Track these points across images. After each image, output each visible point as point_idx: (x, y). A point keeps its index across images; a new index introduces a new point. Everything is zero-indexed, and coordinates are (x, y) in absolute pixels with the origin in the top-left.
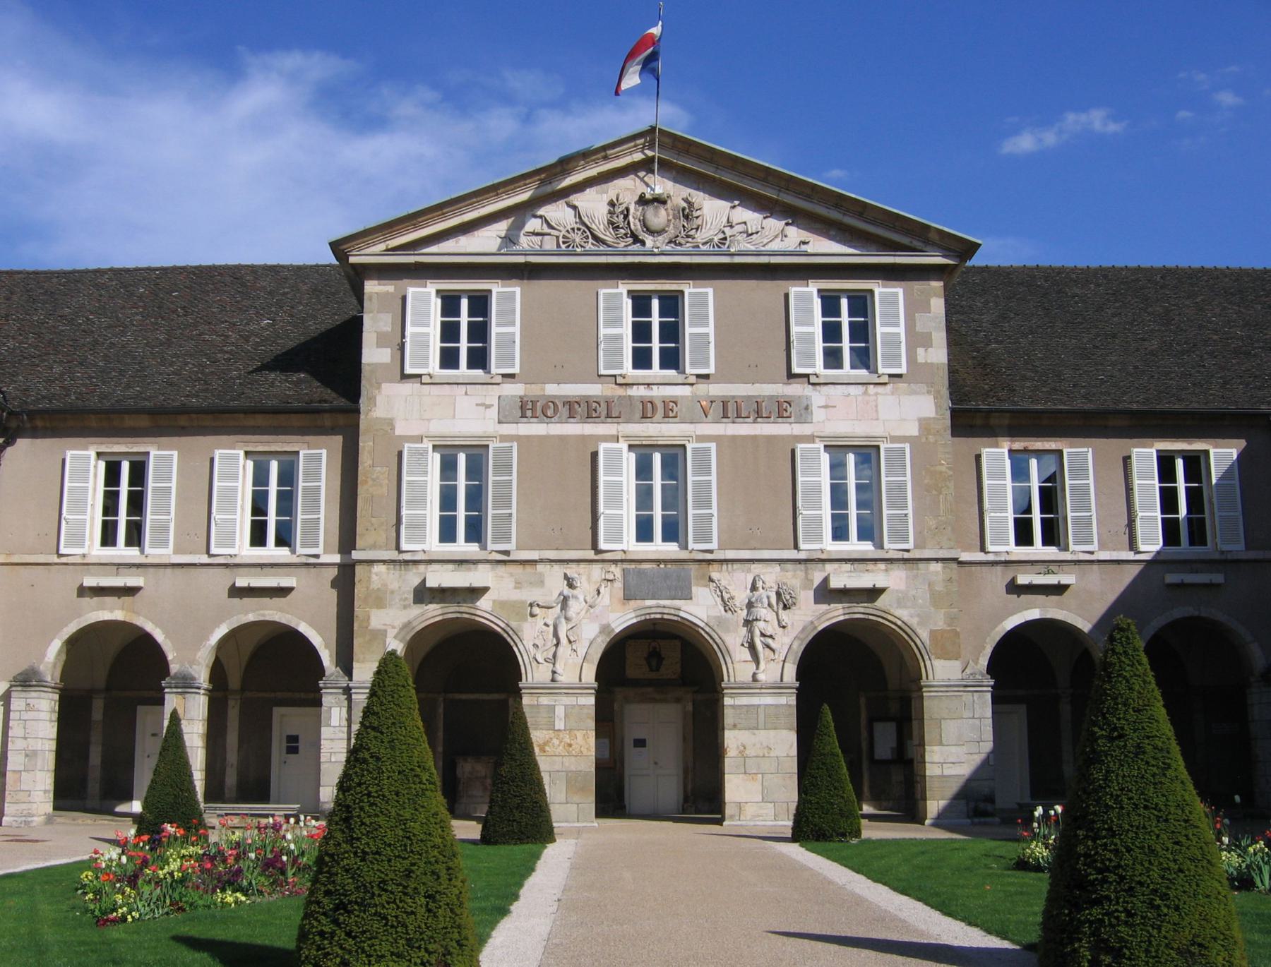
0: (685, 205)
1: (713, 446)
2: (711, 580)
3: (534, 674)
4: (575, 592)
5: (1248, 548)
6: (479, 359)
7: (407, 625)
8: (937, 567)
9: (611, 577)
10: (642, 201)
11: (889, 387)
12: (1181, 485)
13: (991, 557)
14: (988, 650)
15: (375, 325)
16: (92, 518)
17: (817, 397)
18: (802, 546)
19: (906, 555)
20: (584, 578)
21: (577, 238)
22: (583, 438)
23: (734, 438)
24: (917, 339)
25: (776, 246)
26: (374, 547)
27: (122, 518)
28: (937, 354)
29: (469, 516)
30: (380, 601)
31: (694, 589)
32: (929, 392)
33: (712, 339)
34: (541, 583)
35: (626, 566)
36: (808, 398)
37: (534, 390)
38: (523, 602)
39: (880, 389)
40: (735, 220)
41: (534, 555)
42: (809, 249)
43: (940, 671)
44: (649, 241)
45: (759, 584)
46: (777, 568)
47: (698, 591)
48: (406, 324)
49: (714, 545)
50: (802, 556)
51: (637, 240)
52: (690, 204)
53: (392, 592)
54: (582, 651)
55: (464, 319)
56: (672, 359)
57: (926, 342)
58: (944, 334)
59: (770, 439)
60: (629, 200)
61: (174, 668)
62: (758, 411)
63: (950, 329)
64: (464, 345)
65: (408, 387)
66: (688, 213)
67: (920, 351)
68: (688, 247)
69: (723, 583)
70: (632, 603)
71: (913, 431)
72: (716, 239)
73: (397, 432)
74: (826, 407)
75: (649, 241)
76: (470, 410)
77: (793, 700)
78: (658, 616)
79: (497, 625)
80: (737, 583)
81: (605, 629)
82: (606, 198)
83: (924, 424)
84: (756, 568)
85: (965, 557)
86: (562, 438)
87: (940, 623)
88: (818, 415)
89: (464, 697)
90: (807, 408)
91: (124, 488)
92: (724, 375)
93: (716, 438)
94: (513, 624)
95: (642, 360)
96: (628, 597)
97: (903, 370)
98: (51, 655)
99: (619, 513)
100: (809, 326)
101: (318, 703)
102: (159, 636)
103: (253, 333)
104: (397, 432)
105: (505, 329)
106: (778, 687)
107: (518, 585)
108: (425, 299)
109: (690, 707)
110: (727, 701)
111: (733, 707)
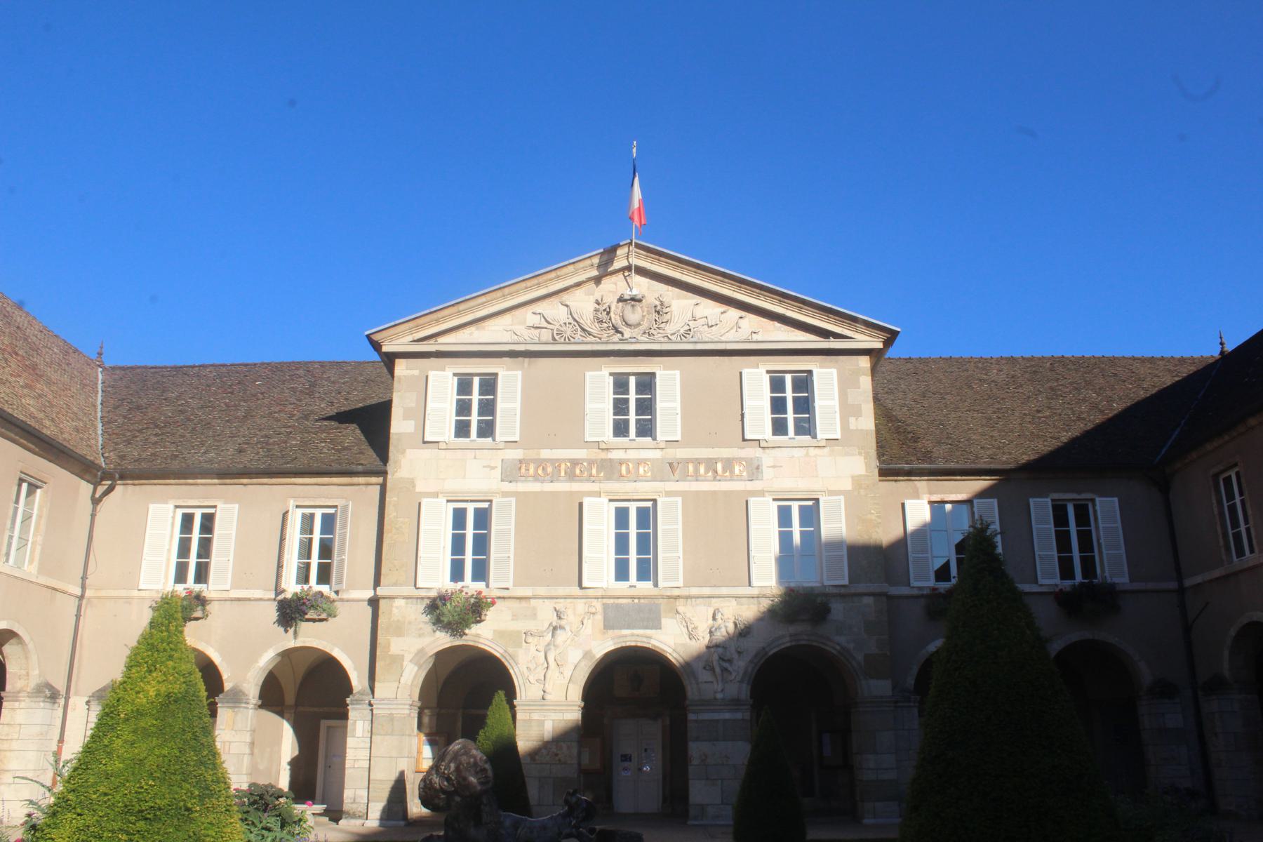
0: (658, 303)
1: (679, 499)
2: (677, 612)
3: (526, 691)
4: (563, 623)
5: (1131, 580)
6: (487, 430)
7: (421, 652)
8: (868, 600)
9: (593, 610)
10: (621, 300)
11: (826, 450)
12: (1073, 528)
13: (915, 592)
16: (168, 560)
17: (767, 459)
18: (754, 583)
19: (843, 591)
20: (570, 612)
21: (568, 331)
22: (571, 493)
24: (848, 410)
25: (731, 336)
26: (395, 584)
27: (193, 560)
28: (867, 422)
30: (399, 630)
31: (664, 621)
32: (860, 454)
33: (679, 410)
34: (534, 616)
35: (605, 601)
36: (758, 459)
37: (532, 454)
38: (519, 632)
39: (818, 451)
40: (698, 315)
44: (628, 333)
45: (718, 616)
46: (733, 602)
47: (667, 622)
48: (425, 402)
49: (680, 584)
50: (755, 592)
51: (618, 331)
52: (662, 304)
53: (410, 623)
54: (568, 674)
55: (475, 397)
56: (646, 429)
57: (857, 413)
58: (871, 405)
60: (611, 300)
61: (227, 686)
63: (876, 399)
64: (474, 418)
65: (427, 453)
66: (660, 310)
67: (852, 420)
68: (659, 337)
69: (688, 615)
70: (610, 632)
71: (848, 485)
72: (682, 331)
73: (418, 489)
74: (774, 467)
75: (628, 333)
76: (476, 472)
77: (747, 716)
78: (633, 644)
79: (497, 651)
81: (587, 654)
82: (592, 299)
83: (856, 480)
84: (716, 603)
85: (895, 591)
86: (554, 494)
88: (767, 473)
89: (316, 709)
90: (758, 468)
91: (196, 535)
92: (688, 440)
93: (683, 494)
94: (510, 650)
95: (620, 429)
97: (838, 436)
101: (344, 716)
103: (312, 412)
104: (418, 489)
105: (509, 403)
106: (735, 703)
107: (515, 617)
108: (442, 383)
109: (668, 722)
110: (691, 717)
111: (696, 721)
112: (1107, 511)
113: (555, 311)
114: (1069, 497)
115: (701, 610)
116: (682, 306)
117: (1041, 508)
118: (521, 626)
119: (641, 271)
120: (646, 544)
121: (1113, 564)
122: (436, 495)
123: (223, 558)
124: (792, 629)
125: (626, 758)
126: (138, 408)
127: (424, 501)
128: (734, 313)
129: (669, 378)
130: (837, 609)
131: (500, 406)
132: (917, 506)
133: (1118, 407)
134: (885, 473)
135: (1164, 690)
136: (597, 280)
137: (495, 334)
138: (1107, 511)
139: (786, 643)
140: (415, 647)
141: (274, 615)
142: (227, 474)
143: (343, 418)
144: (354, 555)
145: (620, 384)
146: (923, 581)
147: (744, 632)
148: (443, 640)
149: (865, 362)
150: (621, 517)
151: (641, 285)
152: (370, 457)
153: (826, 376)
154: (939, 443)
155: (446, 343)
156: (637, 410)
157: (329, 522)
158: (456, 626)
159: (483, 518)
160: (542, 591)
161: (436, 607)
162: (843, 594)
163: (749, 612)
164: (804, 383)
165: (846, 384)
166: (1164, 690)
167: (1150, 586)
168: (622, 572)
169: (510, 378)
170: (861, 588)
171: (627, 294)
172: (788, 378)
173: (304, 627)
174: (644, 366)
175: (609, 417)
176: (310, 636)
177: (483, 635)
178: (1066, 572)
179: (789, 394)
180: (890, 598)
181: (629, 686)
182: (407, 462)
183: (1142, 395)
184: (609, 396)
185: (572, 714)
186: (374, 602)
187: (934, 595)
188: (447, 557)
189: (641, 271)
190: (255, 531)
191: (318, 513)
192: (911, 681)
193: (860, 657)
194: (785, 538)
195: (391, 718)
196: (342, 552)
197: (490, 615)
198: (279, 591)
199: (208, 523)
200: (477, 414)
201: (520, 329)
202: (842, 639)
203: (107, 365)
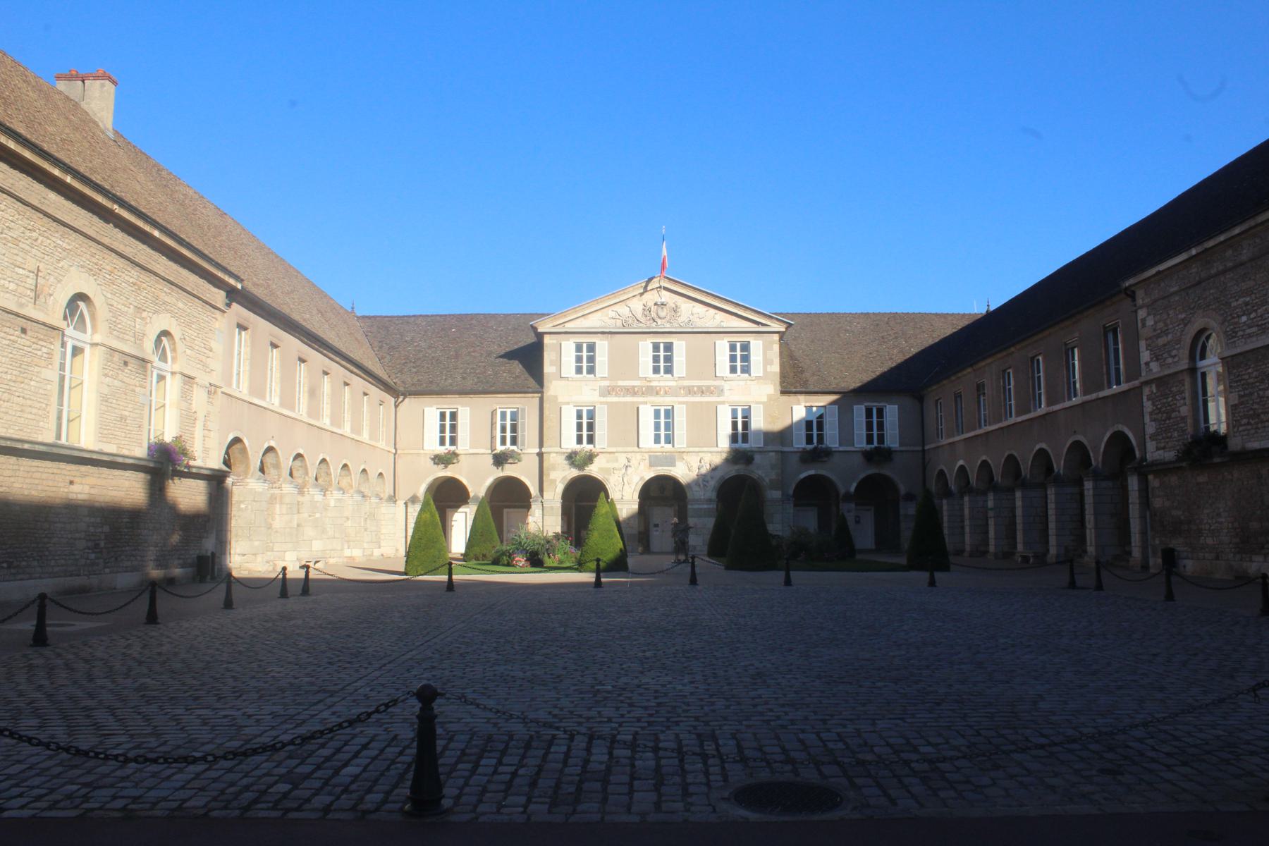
3: (614, 494)
5: (901, 445)
6: (591, 370)
12: (875, 420)
14: (794, 486)
17: (726, 386)
22: (633, 403)
23: (693, 403)
24: (767, 362)
28: (775, 368)
30: (554, 468)
34: (617, 460)
37: (614, 383)
41: (613, 449)
42: (724, 324)
44: (659, 322)
48: (560, 358)
56: (669, 370)
57: (771, 363)
59: (708, 403)
60: (651, 304)
61: (472, 495)
62: (702, 391)
64: (585, 364)
65: (563, 383)
71: (765, 399)
75: (659, 322)
79: (600, 477)
83: (770, 397)
85: (786, 449)
87: (773, 475)
88: (726, 393)
91: (448, 423)
92: (688, 377)
95: (656, 370)
96: (651, 465)
98: (421, 491)
101: (528, 507)
102: (465, 482)
104: (560, 399)
106: (710, 500)
108: (569, 346)
112: (892, 412)
113: (623, 310)
114: (875, 405)
115: (697, 458)
116: (686, 307)
117: (859, 411)
118: (611, 465)
119: (666, 289)
120: (669, 426)
121: (892, 440)
122: (568, 403)
123: (466, 435)
124: (737, 467)
125: (656, 526)
126: (393, 348)
127: (564, 407)
128: (712, 311)
129: (680, 346)
130: (757, 458)
131: (598, 359)
132: (799, 410)
133: (914, 351)
134: (783, 392)
135: (910, 497)
136: (642, 294)
137: (593, 322)
138: (892, 412)
139: (733, 473)
140: (561, 475)
141: (491, 461)
142: (463, 392)
143: (510, 355)
144: (529, 431)
145: (656, 347)
146: (800, 443)
147: (714, 469)
148: (574, 473)
149: (776, 337)
150: (657, 413)
151: (666, 297)
152: (531, 382)
153: (756, 345)
154: (813, 374)
155: (570, 326)
156: (664, 360)
157: (514, 417)
158: (581, 467)
159: (591, 415)
160: (620, 449)
161: (571, 458)
162: (761, 451)
163: (718, 459)
164: (746, 347)
165: (766, 348)
166: (910, 497)
167: (912, 448)
168: (657, 440)
169: (602, 345)
170: (769, 448)
171: (659, 301)
172: (738, 345)
173: (507, 466)
174: (668, 339)
175: (651, 364)
176: (509, 471)
177: (593, 470)
178: (870, 439)
179: (738, 353)
180: (782, 452)
181: (661, 492)
182: (553, 388)
183: (931, 342)
184: (651, 353)
185: (635, 507)
186: (540, 455)
187: (804, 452)
188: (574, 433)
189: (666, 289)
190: (476, 418)
191: (508, 412)
192: (791, 492)
193: (767, 480)
194: (735, 425)
195: (552, 508)
196: (523, 431)
197: (596, 460)
198: (493, 449)
199: (454, 416)
200: (587, 362)
201: (606, 319)
202: (760, 472)
203: (359, 314)
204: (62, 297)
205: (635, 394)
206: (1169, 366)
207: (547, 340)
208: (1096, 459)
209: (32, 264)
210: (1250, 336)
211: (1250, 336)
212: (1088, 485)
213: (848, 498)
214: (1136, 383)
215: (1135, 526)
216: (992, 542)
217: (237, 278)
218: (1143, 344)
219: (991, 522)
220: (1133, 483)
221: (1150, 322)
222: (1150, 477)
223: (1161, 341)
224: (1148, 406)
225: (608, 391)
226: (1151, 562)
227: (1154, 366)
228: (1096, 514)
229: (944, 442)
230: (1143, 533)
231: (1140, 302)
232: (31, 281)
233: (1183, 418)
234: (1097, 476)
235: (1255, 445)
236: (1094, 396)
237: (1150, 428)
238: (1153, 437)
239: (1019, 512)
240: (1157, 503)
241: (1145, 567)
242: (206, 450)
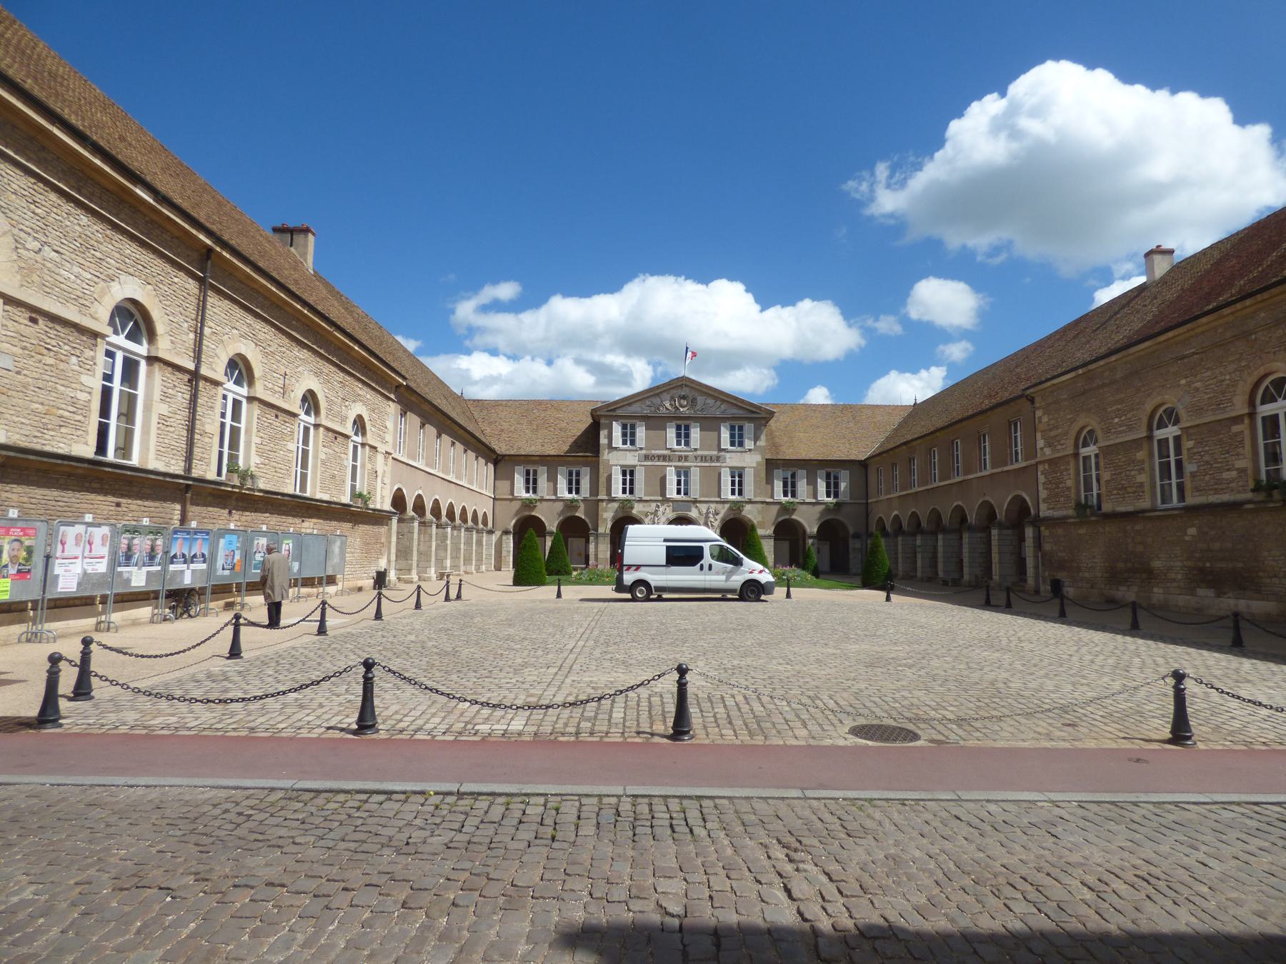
15: (603, 433)
17: (728, 455)
29: (629, 487)
43: (760, 532)
56: (687, 444)
76: (631, 459)
80: (703, 508)
87: (760, 519)
92: (701, 449)
95: (679, 443)
99: (672, 492)
100: (725, 434)
116: (700, 399)
135: (856, 536)
155: (619, 412)
159: (632, 473)
166: (856, 536)
170: (758, 499)
174: (687, 422)
182: (605, 455)
200: (629, 436)
204: (299, 393)
205: (664, 460)
206: (1058, 451)
207: (603, 421)
208: (1001, 515)
209: (282, 369)
210: (1121, 432)
211: (1121, 432)
212: (995, 532)
213: (811, 537)
214: (1033, 462)
215: (1030, 563)
216: (919, 570)
217: (404, 378)
218: (1039, 435)
219: (919, 556)
220: (1029, 532)
221: (1045, 419)
222: (1042, 528)
223: (1053, 433)
224: (1042, 479)
225: (647, 457)
226: (1042, 588)
227: (1048, 451)
228: (1000, 553)
229: (883, 497)
230: (1036, 567)
231: (1037, 405)
232: (281, 382)
233: (1069, 489)
234: (1001, 526)
235: (1122, 509)
236: (1000, 470)
237: (1043, 494)
238: (1044, 500)
239: (940, 549)
240: (1047, 547)
241: (1037, 592)
242: (383, 497)
